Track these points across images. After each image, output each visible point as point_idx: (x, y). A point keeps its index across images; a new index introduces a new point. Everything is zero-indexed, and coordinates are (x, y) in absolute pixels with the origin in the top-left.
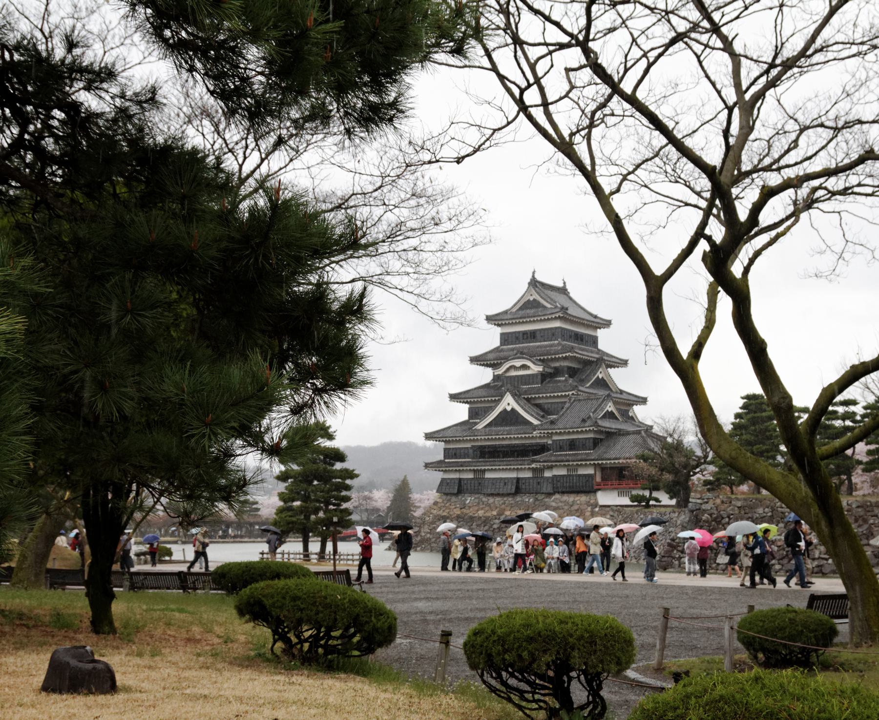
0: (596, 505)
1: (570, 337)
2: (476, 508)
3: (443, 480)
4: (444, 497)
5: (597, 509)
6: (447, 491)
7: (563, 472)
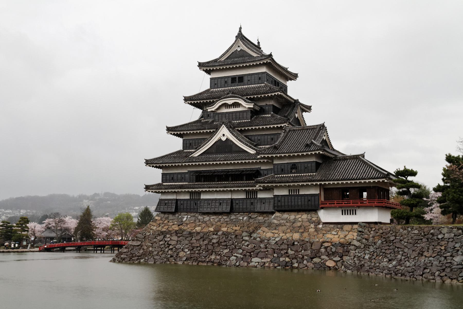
0: (319, 222)
2: (193, 225)
3: (161, 200)
4: (162, 215)
5: (320, 226)
6: (166, 210)
7: (285, 192)
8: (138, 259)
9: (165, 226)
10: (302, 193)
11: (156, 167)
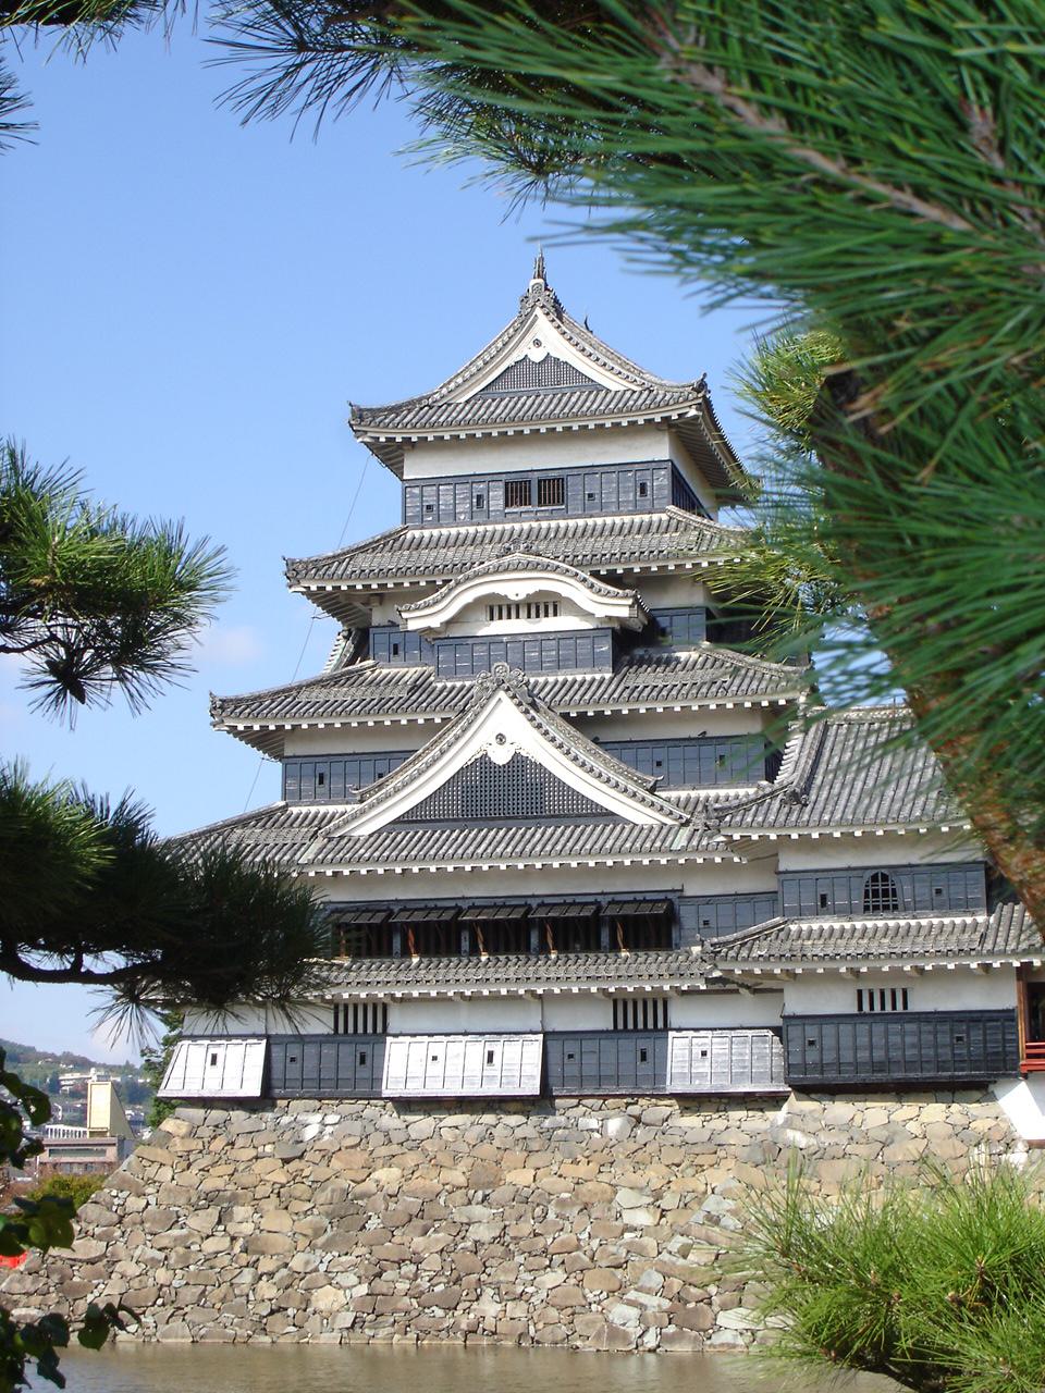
2: (359, 1157)
9: (214, 1164)
10: (916, 1005)
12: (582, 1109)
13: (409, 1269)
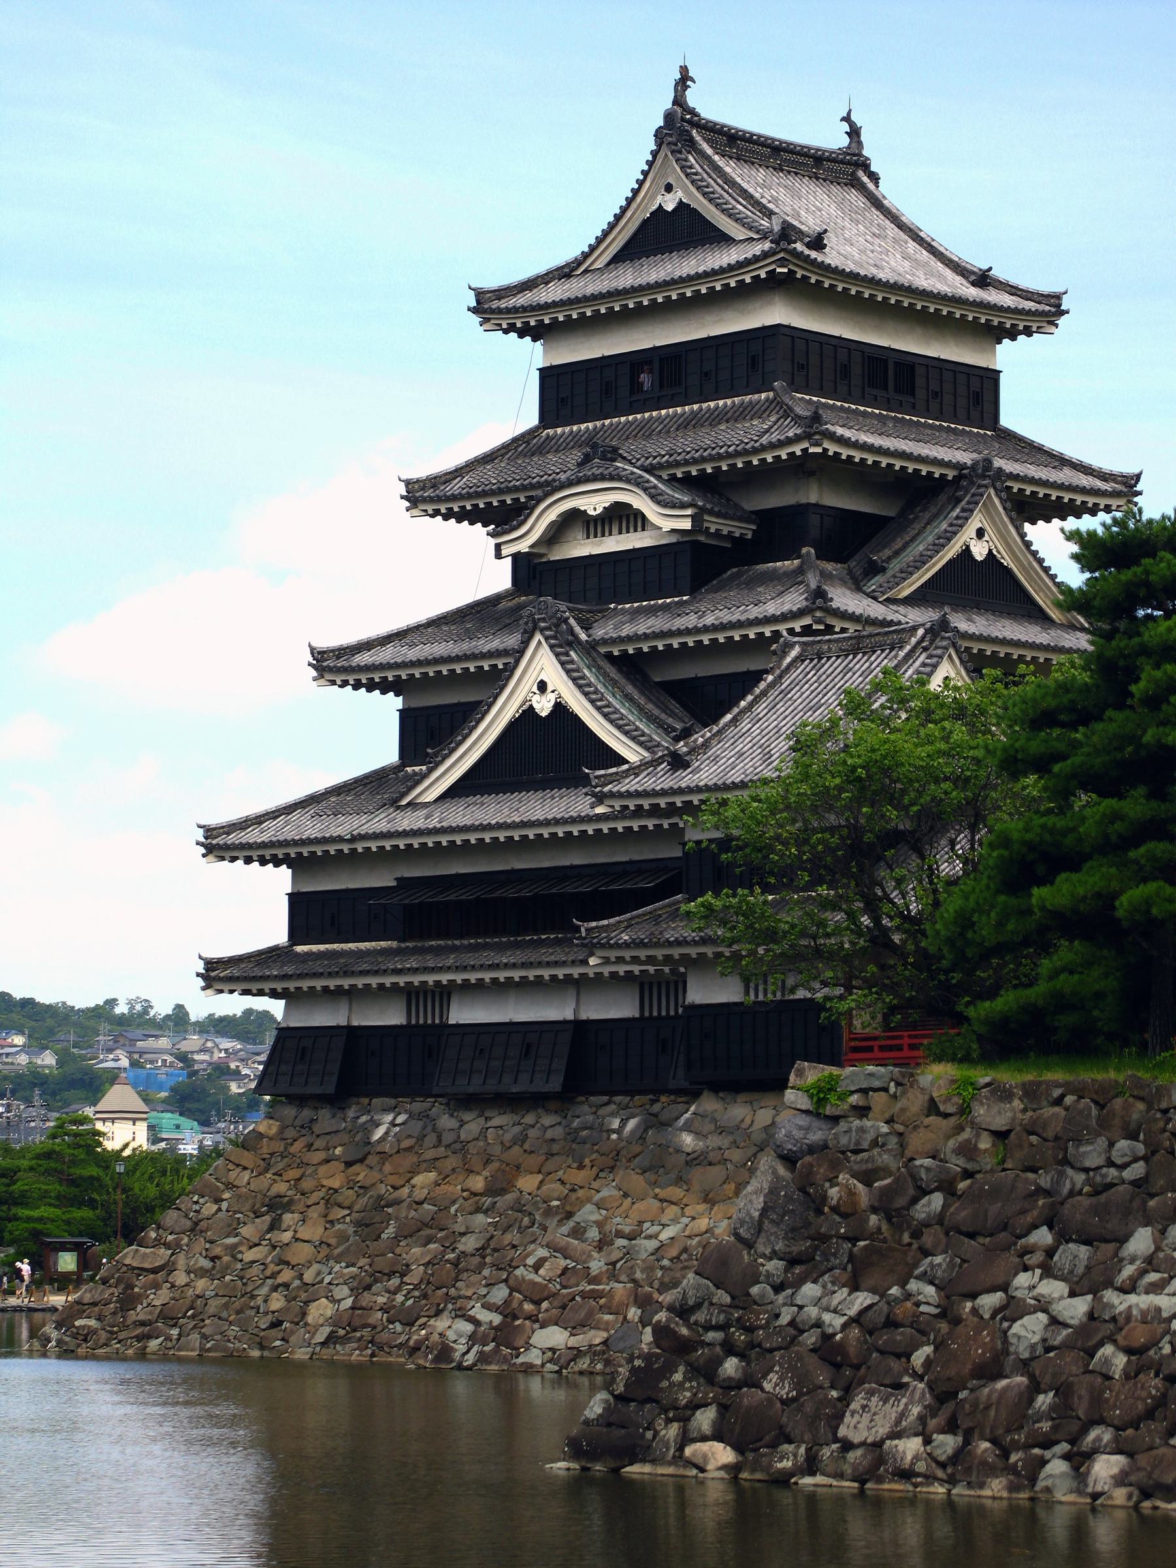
1: (845, 372)
2: (412, 1159)
8: (139, 1338)
11: (263, 862)
12: (613, 1107)
13: (395, 1282)
